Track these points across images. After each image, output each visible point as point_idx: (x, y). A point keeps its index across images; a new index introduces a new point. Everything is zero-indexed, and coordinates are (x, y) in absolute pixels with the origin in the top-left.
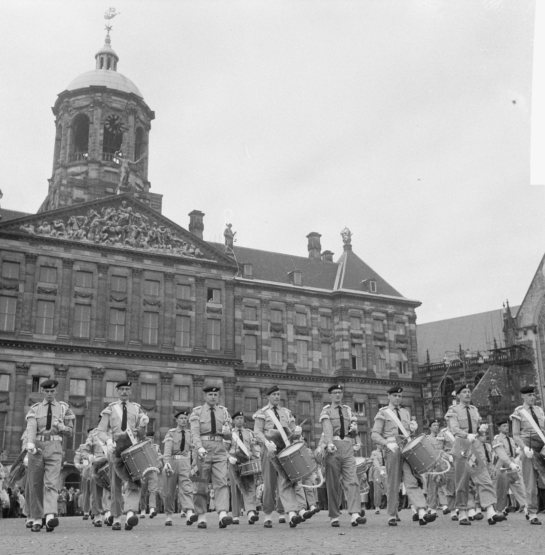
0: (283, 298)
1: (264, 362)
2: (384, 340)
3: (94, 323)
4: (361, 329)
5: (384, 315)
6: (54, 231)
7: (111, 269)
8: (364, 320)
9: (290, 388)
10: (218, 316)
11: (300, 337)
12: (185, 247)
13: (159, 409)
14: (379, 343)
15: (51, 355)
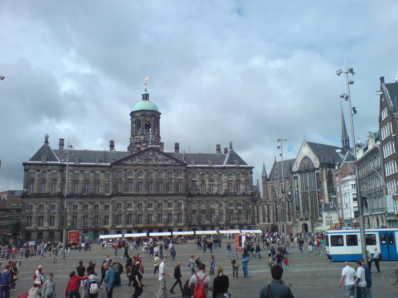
0: (205, 171)
1: (198, 192)
2: (240, 181)
3: (144, 187)
4: (232, 178)
5: (240, 173)
6: (131, 161)
7: (148, 170)
8: (233, 175)
9: (208, 200)
10: (181, 181)
11: (211, 183)
12: (170, 161)
13: (164, 211)
14: (239, 182)
15: (133, 197)
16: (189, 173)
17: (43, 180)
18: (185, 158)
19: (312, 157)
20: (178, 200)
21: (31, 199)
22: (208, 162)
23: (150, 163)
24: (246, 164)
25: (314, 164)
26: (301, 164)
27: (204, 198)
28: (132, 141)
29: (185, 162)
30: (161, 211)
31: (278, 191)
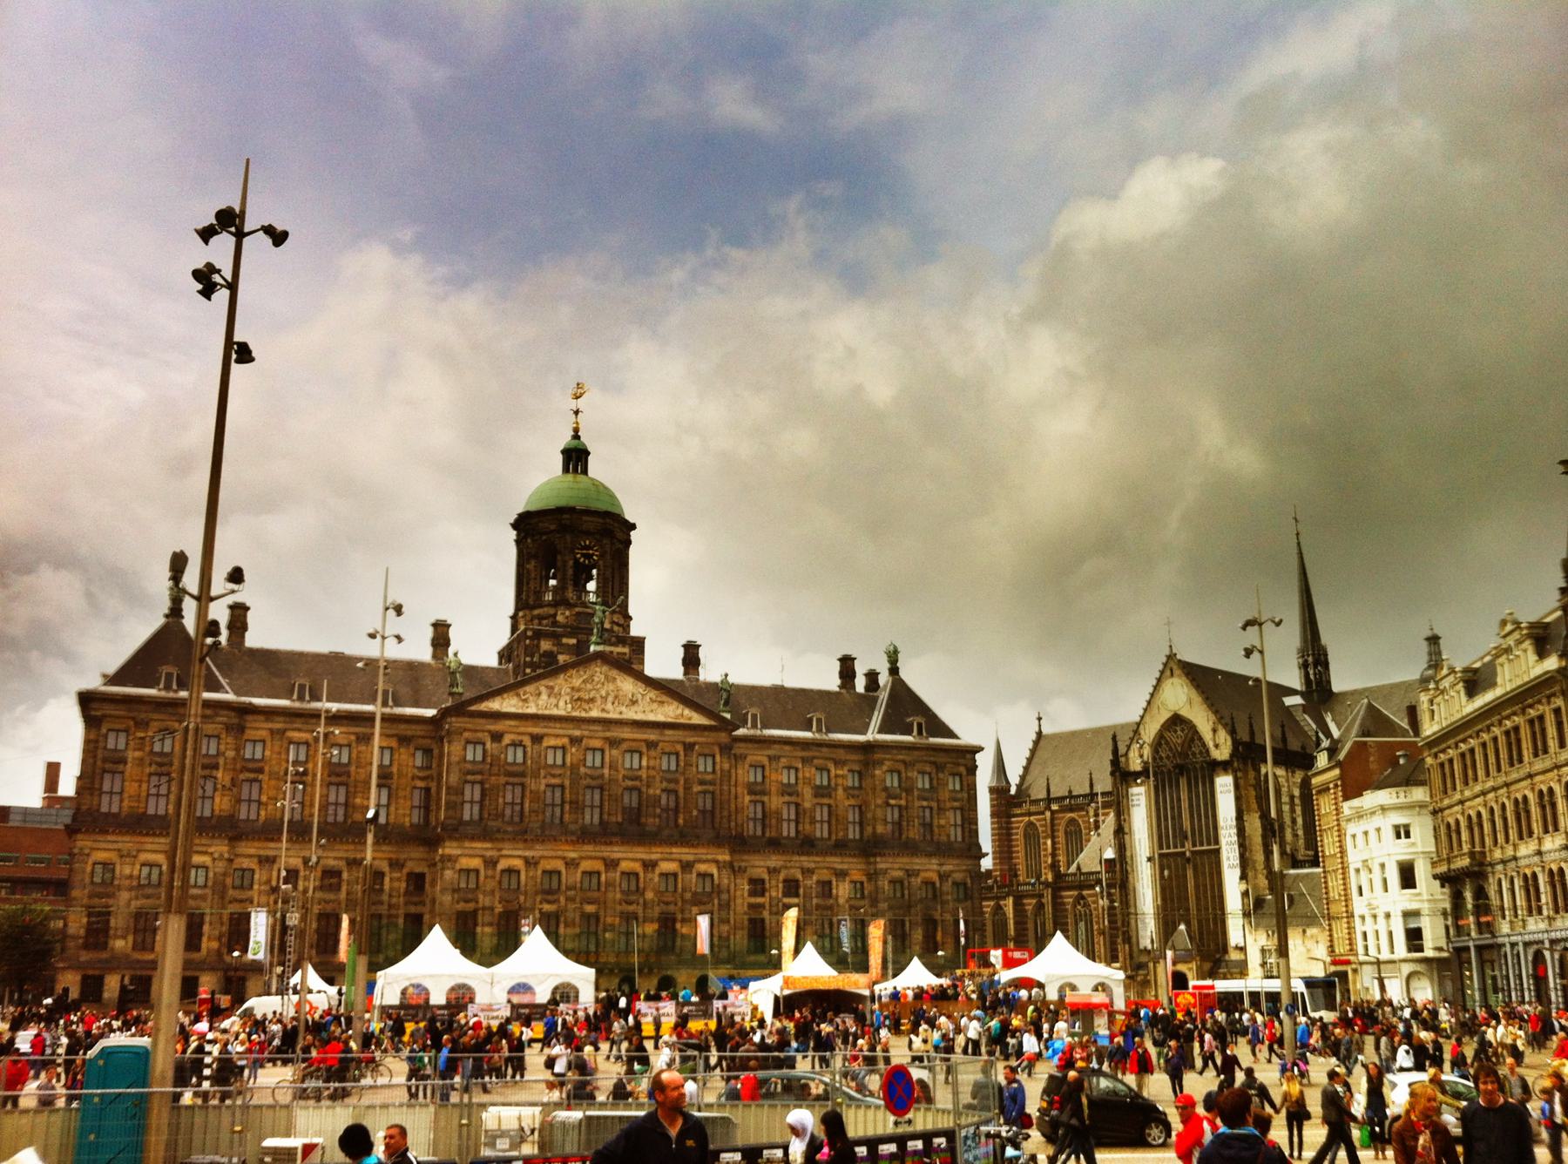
9: (806, 865)
16: (740, 758)
17: (160, 765)
18: (726, 703)
19: (1202, 720)
20: (700, 861)
21: (110, 838)
22: (810, 720)
23: (595, 713)
24: (951, 734)
25: (1211, 745)
26: (1159, 744)
27: (796, 858)
28: (522, 627)
29: (728, 716)
30: (630, 903)
31: (1054, 843)
